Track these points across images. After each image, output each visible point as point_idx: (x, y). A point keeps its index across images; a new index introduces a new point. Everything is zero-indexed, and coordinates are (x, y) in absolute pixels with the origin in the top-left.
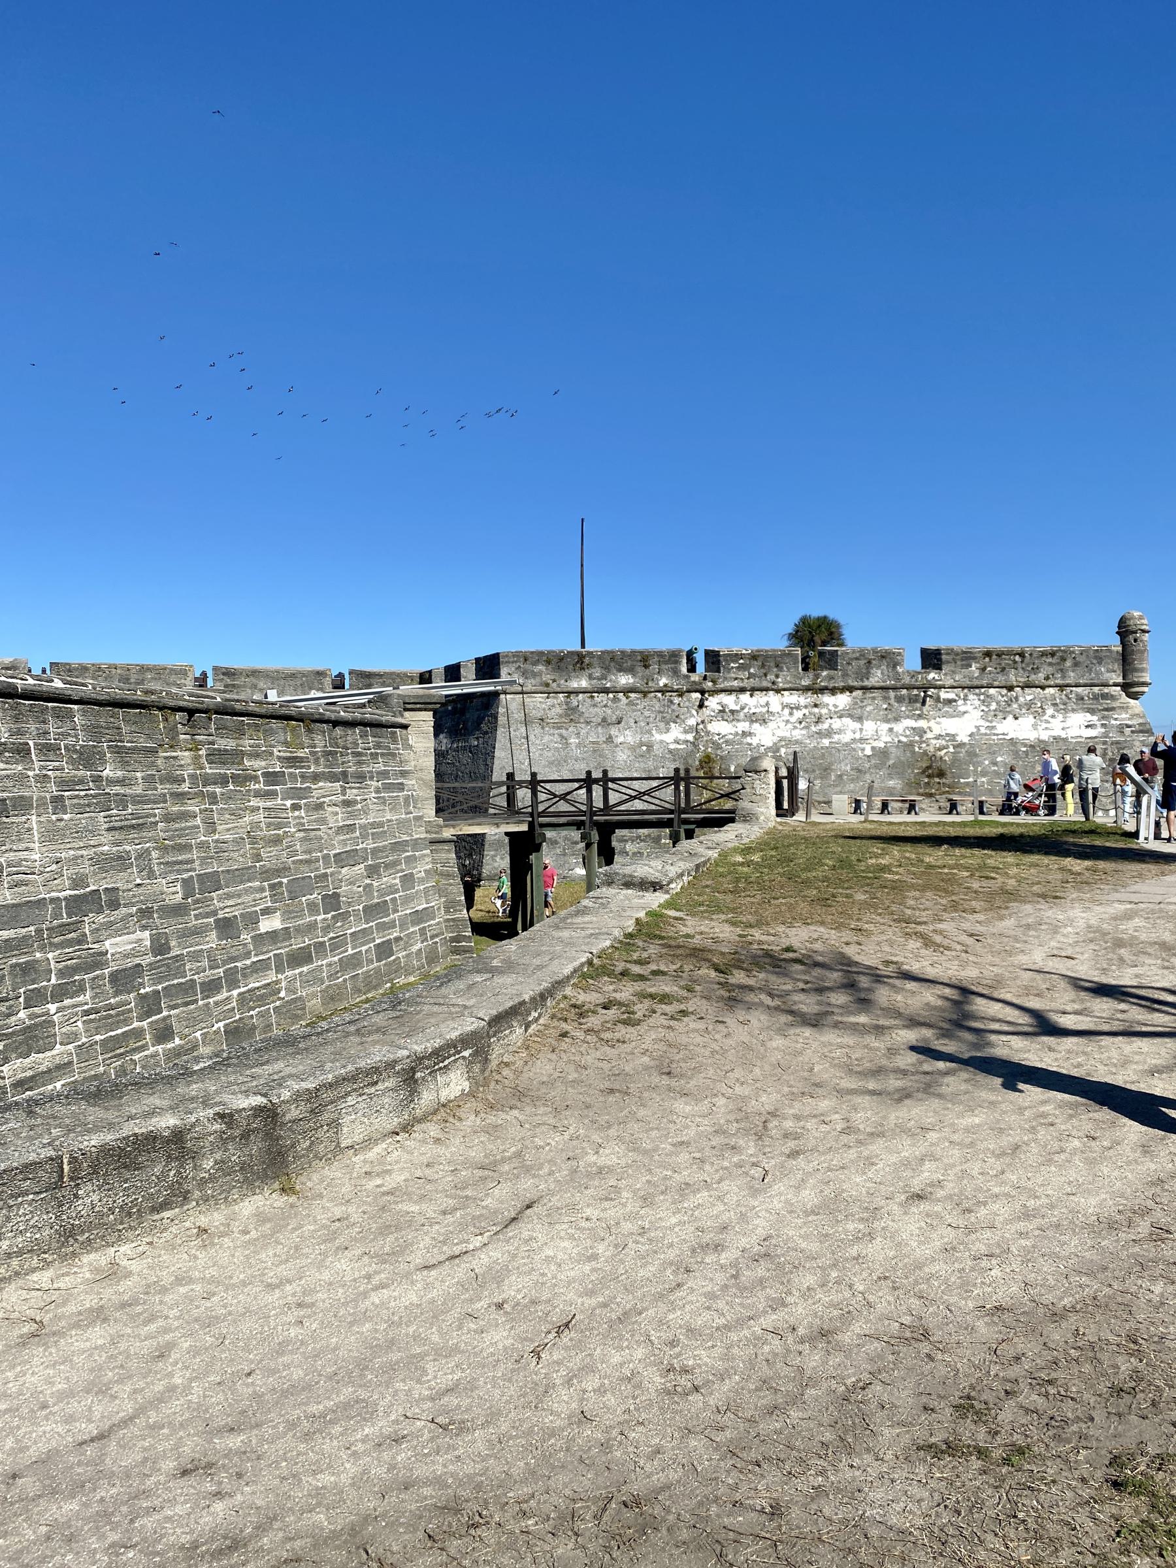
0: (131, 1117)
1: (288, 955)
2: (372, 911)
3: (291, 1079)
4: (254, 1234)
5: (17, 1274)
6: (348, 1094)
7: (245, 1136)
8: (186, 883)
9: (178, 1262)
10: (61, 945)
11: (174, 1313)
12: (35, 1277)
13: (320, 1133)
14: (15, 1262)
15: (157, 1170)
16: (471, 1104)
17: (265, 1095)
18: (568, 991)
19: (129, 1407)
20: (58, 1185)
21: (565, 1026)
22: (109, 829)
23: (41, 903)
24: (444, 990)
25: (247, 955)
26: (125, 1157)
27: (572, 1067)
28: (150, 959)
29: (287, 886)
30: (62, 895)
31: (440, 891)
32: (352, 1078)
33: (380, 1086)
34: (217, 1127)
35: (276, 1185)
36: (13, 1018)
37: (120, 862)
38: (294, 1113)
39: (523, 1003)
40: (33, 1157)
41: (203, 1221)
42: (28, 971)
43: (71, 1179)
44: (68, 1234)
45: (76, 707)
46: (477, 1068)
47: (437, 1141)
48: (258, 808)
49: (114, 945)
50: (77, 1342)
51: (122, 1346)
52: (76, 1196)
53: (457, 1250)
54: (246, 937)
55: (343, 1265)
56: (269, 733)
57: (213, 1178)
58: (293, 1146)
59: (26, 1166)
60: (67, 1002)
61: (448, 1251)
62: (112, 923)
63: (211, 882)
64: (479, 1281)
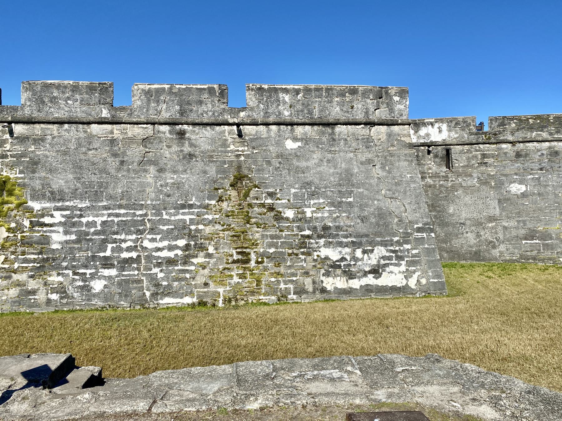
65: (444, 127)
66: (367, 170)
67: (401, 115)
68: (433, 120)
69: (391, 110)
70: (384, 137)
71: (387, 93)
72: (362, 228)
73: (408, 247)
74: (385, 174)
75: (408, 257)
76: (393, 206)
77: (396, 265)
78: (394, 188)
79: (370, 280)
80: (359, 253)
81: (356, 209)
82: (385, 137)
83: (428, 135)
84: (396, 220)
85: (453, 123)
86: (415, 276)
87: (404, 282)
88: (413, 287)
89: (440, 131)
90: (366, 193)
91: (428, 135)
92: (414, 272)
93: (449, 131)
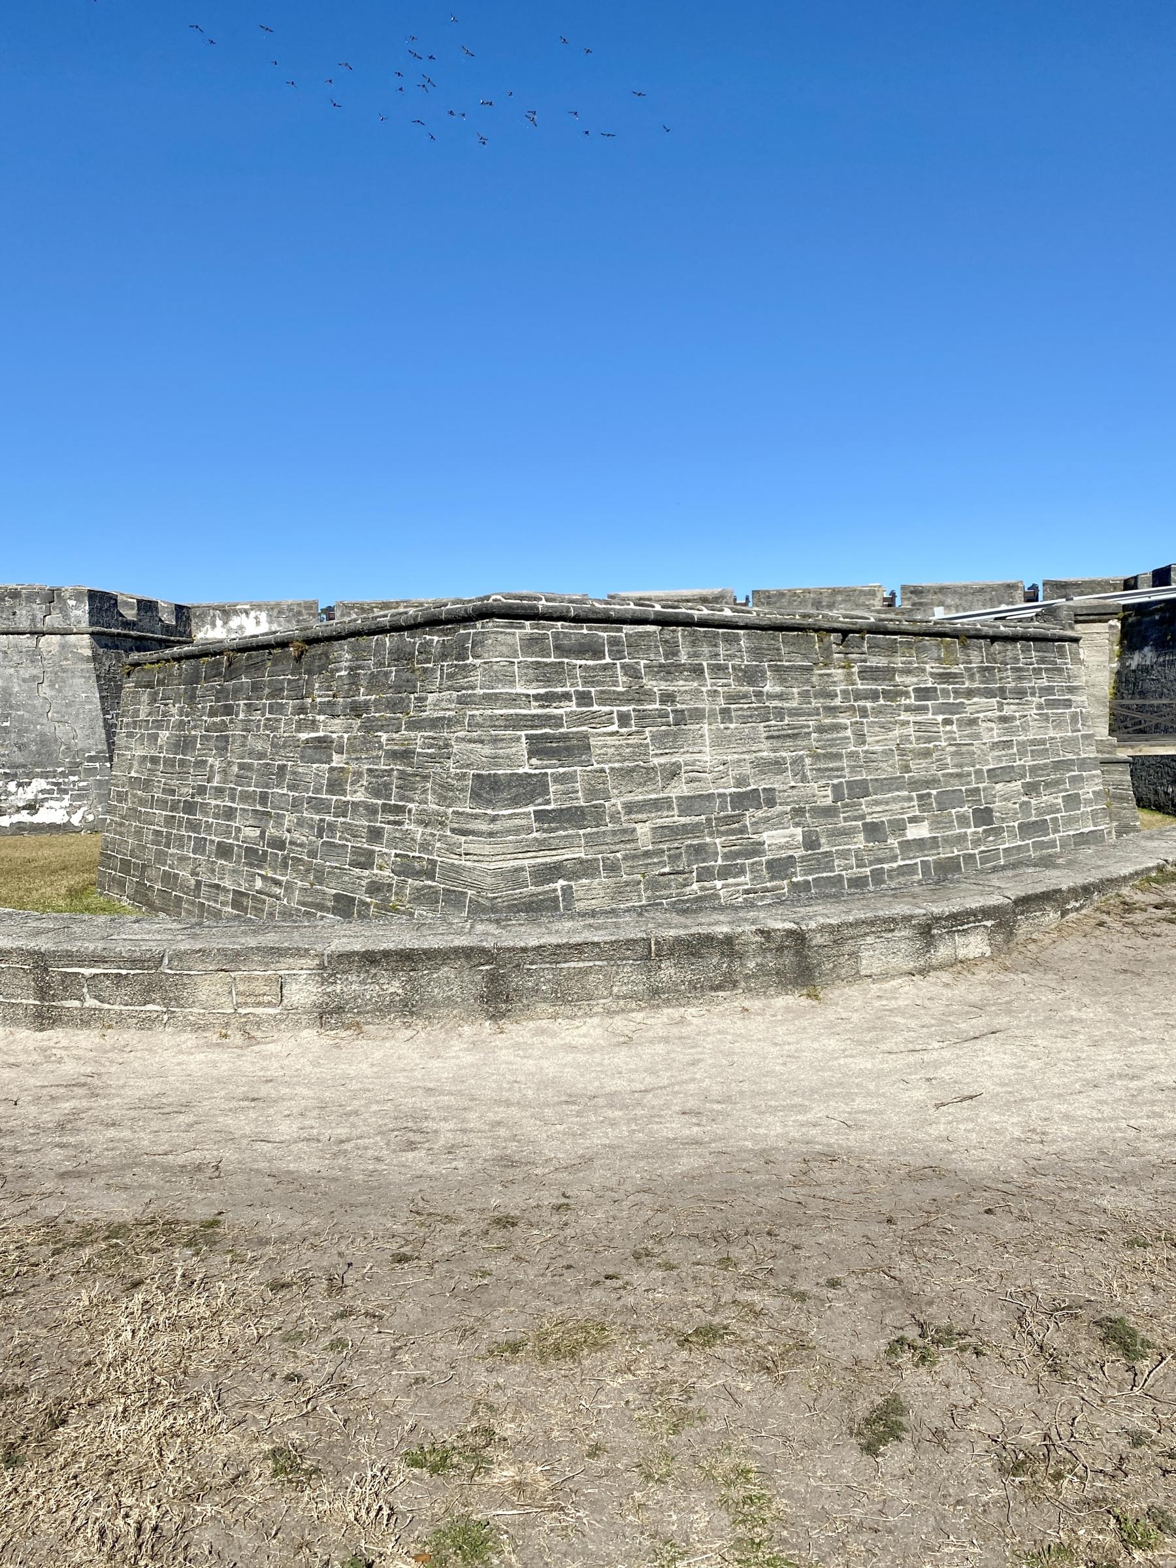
0: (701, 924)
1: (935, 862)
2: (1026, 829)
3: (820, 916)
4: (779, 1017)
5: (623, 1010)
6: (866, 934)
7: (780, 949)
8: (836, 787)
9: (725, 1024)
10: (723, 834)
11: (710, 1046)
12: (634, 1014)
13: (842, 960)
14: (622, 1002)
15: (715, 961)
16: (990, 965)
17: (797, 924)
18: (1125, 891)
19: (666, 1082)
20: (648, 957)
21: (1105, 917)
22: (768, 738)
23: (710, 796)
24: (991, 876)
25: (894, 858)
26: (694, 948)
27: (1097, 950)
28: (801, 852)
29: (937, 798)
30: (728, 791)
31: (1110, 814)
32: (872, 923)
33: (896, 933)
34: (758, 939)
35: (805, 992)
36: (688, 889)
37: (777, 766)
38: (818, 940)
39: (1060, 890)
40: (632, 936)
41: (746, 1004)
42: (699, 851)
43: (657, 955)
44: (655, 992)
45: (742, 632)
46: (1000, 938)
47: (947, 985)
48: (908, 722)
49: (772, 837)
50: (647, 1051)
51: (672, 1055)
52: (659, 967)
53: (918, 1047)
54: (893, 842)
55: (832, 1043)
56: (921, 650)
57: (754, 976)
58: (819, 965)
59: (628, 941)
60: (731, 881)
61: (911, 1046)
62: (768, 819)
63: (860, 789)
64: (923, 1064)
65: (263, 616)
66: (31, 689)
67: (79, 622)
68: (247, 607)
69: (66, 617)
70: (55, 649)
71: (59, 596)
72: (19, 757)
73: (76, 778)
74: (53, 693)
75: (73, 790)
76: (62, 731)
77: (57, 799)
78: (64, 710)
79: (24, 817)
80: (12, 787)
81: (13, 736)
82: (57, 649)
83: (241, 628)
84: (63, 747)
85: (275, 611)
86: (80, 813)
87: (66, 819)
88: (77, 824)
89: (258, 623)
90: (27, 715)
91: (241, 628)
92: (80, 807)
93: (270, 622)
